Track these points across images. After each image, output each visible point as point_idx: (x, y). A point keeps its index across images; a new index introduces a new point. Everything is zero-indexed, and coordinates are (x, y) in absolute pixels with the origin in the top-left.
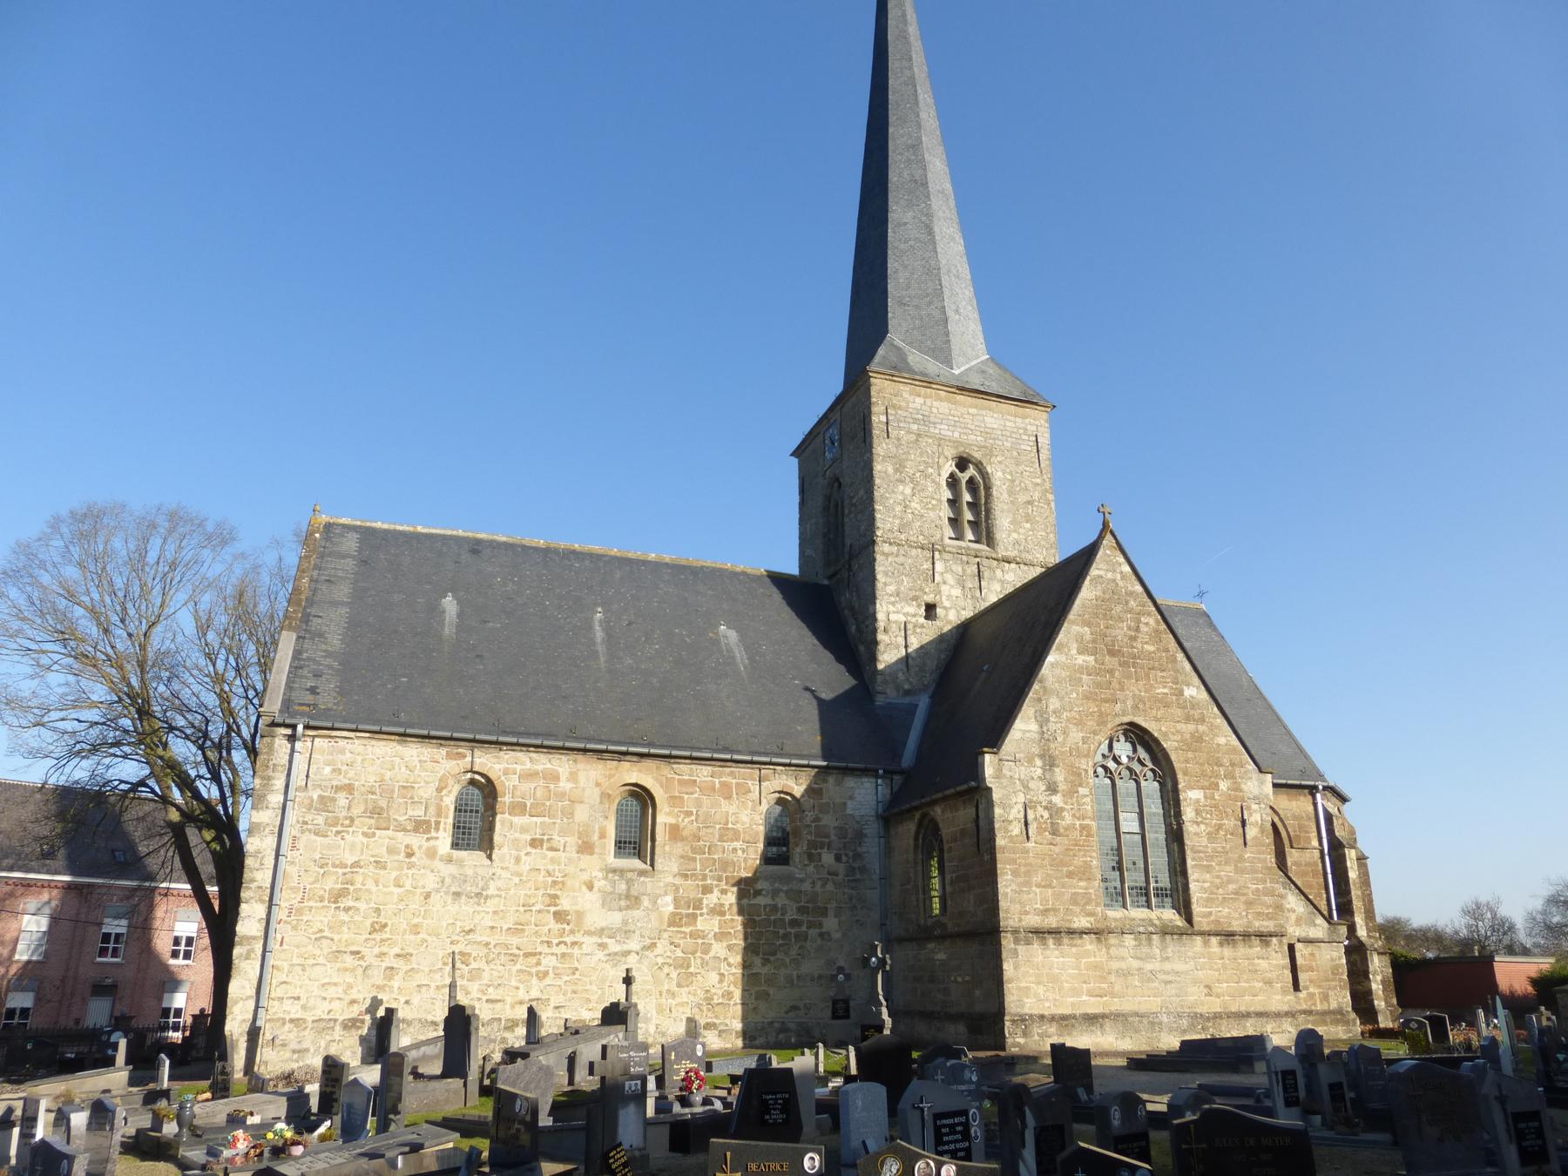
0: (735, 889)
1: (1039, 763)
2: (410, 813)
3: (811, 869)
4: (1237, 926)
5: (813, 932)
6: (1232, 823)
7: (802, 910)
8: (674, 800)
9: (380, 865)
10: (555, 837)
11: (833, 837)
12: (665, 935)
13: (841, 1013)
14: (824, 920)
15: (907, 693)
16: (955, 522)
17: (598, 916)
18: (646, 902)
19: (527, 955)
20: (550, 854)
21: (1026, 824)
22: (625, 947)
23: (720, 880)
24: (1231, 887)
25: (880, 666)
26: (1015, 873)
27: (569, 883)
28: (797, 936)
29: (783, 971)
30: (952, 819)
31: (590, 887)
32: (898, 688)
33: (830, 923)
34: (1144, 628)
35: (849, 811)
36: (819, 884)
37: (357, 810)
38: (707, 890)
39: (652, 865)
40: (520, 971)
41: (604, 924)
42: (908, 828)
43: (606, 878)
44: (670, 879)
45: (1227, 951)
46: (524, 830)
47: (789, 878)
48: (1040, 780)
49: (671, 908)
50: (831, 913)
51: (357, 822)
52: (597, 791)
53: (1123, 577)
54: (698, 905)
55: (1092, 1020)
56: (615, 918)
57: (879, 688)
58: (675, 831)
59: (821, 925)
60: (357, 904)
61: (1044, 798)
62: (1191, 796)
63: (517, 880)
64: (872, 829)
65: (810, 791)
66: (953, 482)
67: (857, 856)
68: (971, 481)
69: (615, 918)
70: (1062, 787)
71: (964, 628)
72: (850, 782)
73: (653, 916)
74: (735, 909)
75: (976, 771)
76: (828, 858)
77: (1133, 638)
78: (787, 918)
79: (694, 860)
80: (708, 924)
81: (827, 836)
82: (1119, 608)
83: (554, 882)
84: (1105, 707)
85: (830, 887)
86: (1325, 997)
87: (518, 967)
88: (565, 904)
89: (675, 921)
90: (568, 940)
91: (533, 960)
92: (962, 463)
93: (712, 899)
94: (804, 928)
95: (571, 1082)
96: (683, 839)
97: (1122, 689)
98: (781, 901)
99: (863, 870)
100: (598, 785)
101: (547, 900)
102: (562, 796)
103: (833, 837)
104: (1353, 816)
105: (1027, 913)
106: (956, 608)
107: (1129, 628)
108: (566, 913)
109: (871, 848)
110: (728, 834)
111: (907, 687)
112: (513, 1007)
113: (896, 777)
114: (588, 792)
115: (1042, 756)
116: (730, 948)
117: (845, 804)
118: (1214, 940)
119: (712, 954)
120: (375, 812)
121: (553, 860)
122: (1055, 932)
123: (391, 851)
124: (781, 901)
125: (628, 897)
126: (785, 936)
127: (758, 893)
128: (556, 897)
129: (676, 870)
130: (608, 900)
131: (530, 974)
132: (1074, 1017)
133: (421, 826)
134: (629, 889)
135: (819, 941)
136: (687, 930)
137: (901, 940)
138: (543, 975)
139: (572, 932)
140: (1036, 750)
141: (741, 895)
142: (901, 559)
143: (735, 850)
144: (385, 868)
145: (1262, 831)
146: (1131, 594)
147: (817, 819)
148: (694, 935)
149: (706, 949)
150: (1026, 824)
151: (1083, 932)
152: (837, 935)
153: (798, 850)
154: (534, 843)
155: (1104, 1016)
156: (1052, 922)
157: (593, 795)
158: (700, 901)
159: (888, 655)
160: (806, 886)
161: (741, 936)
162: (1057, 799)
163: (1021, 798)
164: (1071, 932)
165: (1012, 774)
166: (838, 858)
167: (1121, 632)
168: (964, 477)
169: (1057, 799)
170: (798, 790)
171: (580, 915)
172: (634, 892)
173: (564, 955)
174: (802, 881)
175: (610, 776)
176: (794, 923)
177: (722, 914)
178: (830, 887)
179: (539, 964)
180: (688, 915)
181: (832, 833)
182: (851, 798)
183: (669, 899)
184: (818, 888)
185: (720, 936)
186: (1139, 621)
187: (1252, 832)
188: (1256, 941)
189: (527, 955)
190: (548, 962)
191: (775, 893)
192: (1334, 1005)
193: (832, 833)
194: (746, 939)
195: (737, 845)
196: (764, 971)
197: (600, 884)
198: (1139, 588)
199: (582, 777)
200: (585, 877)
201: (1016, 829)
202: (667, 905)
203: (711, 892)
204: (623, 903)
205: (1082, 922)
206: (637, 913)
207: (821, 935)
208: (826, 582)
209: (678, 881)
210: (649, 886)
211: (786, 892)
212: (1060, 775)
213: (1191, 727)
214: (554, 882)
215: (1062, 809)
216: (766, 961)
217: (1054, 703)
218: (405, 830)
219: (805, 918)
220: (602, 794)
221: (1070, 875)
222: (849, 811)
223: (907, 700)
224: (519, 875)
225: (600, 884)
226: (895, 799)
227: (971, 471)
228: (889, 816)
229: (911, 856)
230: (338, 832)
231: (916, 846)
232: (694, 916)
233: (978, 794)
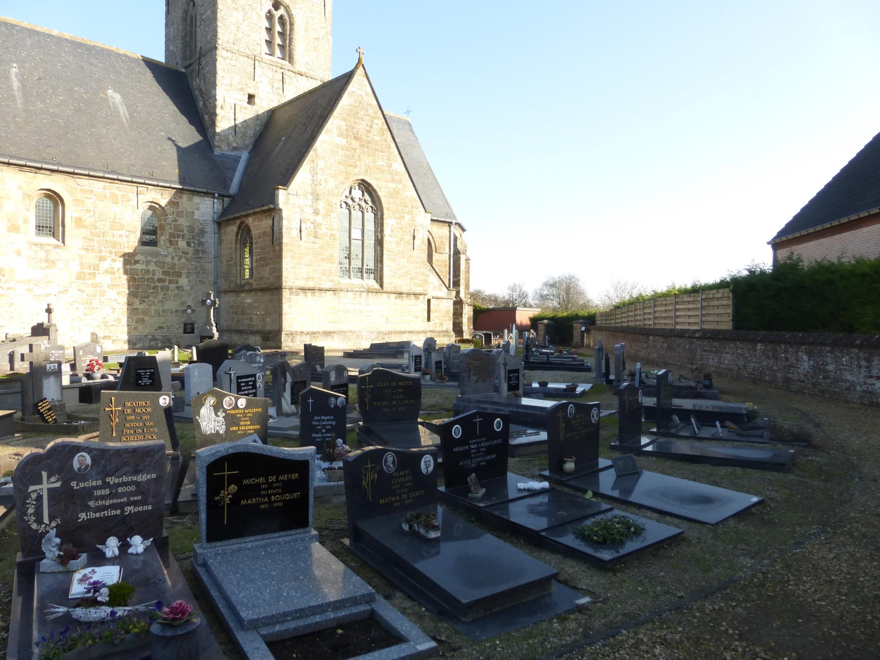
0: (122, 259)
1: (310, 197)
4: (405, 290)
7: (165, 273)
11: (185, 232)
13: (189, 330)
15: (235, 149)
16: (269, 43)
21: (301, 231)
23: (111, 253)
24: (405, 270)
25: (218, 130)
26: (292, 257)
28: (162, 288)
29: (153, 308)
30: (258, 226)
32: (229, 145)
33: (183, 281)
34: (375, 126)
35: (196, 217)
36: (176, 258)
38: (102, 259)
39: (63, 242)
42: (234, 228)
45: (399, 301)
47: (157, 254)
48: (310, 206)
50: (184, 275)
53: (367, 95)
54: (96, 268)
55: (328, 334)
57: (217, 144)
58: (79, 222)
59: (177, 282)
61: (312, 217)
62: (389, 223)
64: (211, 228)
65: (171, 203)
66: (270, 17)
67: (200, 244)
68: (281, 18)
70: (322, 211)
71: (272, 114)
72: (197, 199)
74: (122, 271)
75: (273, 199)
76: (182, 244)
77: (369, 132)
78: (156, 277)
80: (104, 279)
82: (362, 113)
84: (350, 169)
85: (183, 261)
86: (442, 325)
89: (81, 277)
93: (105, 265)
94: (167, 284)
95: (12, 368)
97: (360, 160)
98: (152, 267)
99: (204, 252)
100: (20, 188)
103: (185, 232)
105: (297, 279)
107: (367, 125)
109: (210, 239)
111: (234, 145)
113: (226, 199)
115: (312, 194)
116: (118, 294)
117: (193, 213)
118: (393, 296)
122: (312, 290)
125: (47, 261)
126: (154, 288)
127: (136, 262)
132: (319, 333)
136: (90, 282)
137: (226, 292)
139: (7, 281)
140: (310, 190)
141: (126, 263)
142: (233, 62)
143: (120, 236)
145: (423, 242)
146: (370, 105)
147: (175, 220)
149: (103, 294)
150: (301, 231)
153: (163, 238)
155: (334, 332)
156: (311, 284)
158: (98, 265)
159: (223, 123)
160: (168, 260)
161: (126, 287)
162: (319, 219)
163: (298, 217)
164: (320, 290)
166: (188, 244)
167: (362, 127)
168: (277, 14)
169: (319, 219)
170: (163, 202)
172: (51, 258)
174: (165, 256)
176: (160, 280)
177: (113, 273)
178: (183, 261)
180: (90, 274)
185: (112, 286)
186: (373, 122)
188: (412, 297)
191: (148, 263)
192: (444, 329)
194: (129, 288)
195: (122, 232)
196: (141, 307)
198: (375, 103)
201: (296, 232)
204: (44, 265)
205: (326, 285)
207: (178, 288)
208: (183, 70)
209: (83, 252)
211: (155, 263)
212: (321, 205)
213: (394, 185)
215: (321, 224)
216: (142, 302)
217: (321, 164)
219: (167, 278)
221: (323, 260)
222: (196, 217)
223: (234, 153)
226: (225, 211)
227: (282, 11)
228: (221, 222)
229: (233, 246)
231: (237, 240)
232: (94, 274)
233: (273, 211)
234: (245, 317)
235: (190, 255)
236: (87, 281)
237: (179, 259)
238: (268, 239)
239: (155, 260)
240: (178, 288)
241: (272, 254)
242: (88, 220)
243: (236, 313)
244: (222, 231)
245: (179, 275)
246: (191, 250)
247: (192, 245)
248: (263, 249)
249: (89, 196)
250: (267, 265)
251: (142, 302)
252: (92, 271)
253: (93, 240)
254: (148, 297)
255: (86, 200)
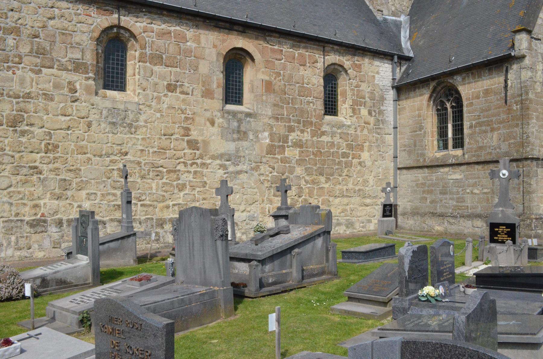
2: (70, 55)
3: (354, 119)
5: (355, 161)
8: (268, 64)
9: (49, 97)
10: (186, 84)
11: (367, 99)
12: (264, 160)
14: (362, 154)
17: (220, 145)
18: (251, 137)
19: (169, 172)
20: (182, 96)
22: (239, 168)
23: (299, 122)
26: (538, 118)
27: (197, 119)
28: (346, 163)
29: (338, 187)
31: (213, 123)
36: (359, 129)
37: (25, 49)
38: (291, 129)
40: (164, 184)
41: (222, 151)
43: (223, 117)
44: (266, 120)
46: (162, 77)
47: (341, 126)
49: (268, 141)
50: (366, 148)
51: (26, 60)
52: (214, 51)
54: (285, 139)
56: (230, 147)
59: (359, 157)
60: (32, 129)
63: (158, 115)
69: (230, 147)
73: (257, 146)
76: (364, 112)
78: (340, 151)
79: (282, 107)
81: (364, 98)
83: (187, 119)
85: (365, 132)
87: (164, 180)
88: (194, 134)
89: (271, 150)
90: (199, 161)
91: (174, 176)
94: (350, 159)
95: (502, 313)
96: (274, 91)
98: (337, 140)
100: (215, 46)
101: (182, 132)
102: (188, 52)
103: (367, 99)
108: (197, 142)
110: (304, 92)
111: (393, 9)
112: (161, 210)
114: (207, 51)
117: (374, 76)
119: (295, 174)
120: (40, 52)
121: (184, 100)
123: (57, 86)
124: (337, 140)
125: (239, 132)
126: (339, 163)
128: (188, 129)
129: (270, 113)
130: (225, 134)
131: (172, 185)
134: (239, 127)
135: (359, 168)
136: (279, 157)
138: (182, 187)
143: (309, 103)
144: (52, 100)
148: (284, 160)
152: (369, 163)
153: (346, 106)
154: (171, 88)
158: (287, 137)
160: (351, 131)
166: (370, 113)
171: (206, 143)
172: (243, 129)
173: (195, 172)
174: (349, 126)
175: (224, 41)
176: (345, 155)
178: (365, 132)
179: (179, 179)
180: (279, 147)
181: (367, 95)
182: (378, 73)
183: (266, 134)
184: (358, 132)
185: (300, 162)
189: (169, 172)
190: (186, 178)
191: (333, 134)
193: (367, 95)
195: (310, 99)
196: (326, 186)
197: (219, 121)
199: (203, 38)
200: (208, 115)
202: (265, 138)
203: (294, 131)
204: (235, 136)
206: (245, 144)
209: (272, 122)
210: (253, 124)
211: (340, 134)
214: (187, 119)
216: (328, 180)
218: (66, 69)
220: (218, 53)
222: (376, 82)
224: (160, 111)
225: (219, 121)
230: (9, 68)
232: (283, 147)
234: (448, 196)
235: (372, 125)
236: (276, 156)
237: (362, 131)
238: (495, 100)
239: (339, 131)
240: (360, 163)
241: (503, 116)
242: (278, 84)
243: (430, 192)
244: (402, 97)
245: (362, 149)
246: (372, 120)
247: (373, 114)
248: (483, 111)
249: (279, 57)
250: (492, 130)
251: (328, 180)
252: (281, 144)
253: (282, 107)
254: (332, 175)
255: (277, 62)
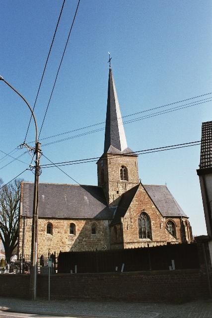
4: (159, 240)
6: (159, 225)
7: (98, 241)
16: (121, 177)
30: (118, 227)
33: (102, 242)
42: (113, 228)
48: (130, 221)
62: (153, 222)
66: (121, 170)
71: (123, 195)
72: (104, 221)
75: (120, 220)
76: (101, 233)
88: (63, 241)
92: (123, 167)
104: (189, 220)
106: (122, 192)
109: (108, 230)
133: (42, 231)
137: (113, 244)
151: (135, 242)
154: (58, 232)
156: (131, 241)
157: (66, 225)
165: (126, 221)
167: (142, 198)
168: (123, 169)
171: (65, 242)
187: (162, 227)
201: (126, 228)
212: (132, 220)
226: (112, 223)
228: (110, 226)
233: (121, 224)
